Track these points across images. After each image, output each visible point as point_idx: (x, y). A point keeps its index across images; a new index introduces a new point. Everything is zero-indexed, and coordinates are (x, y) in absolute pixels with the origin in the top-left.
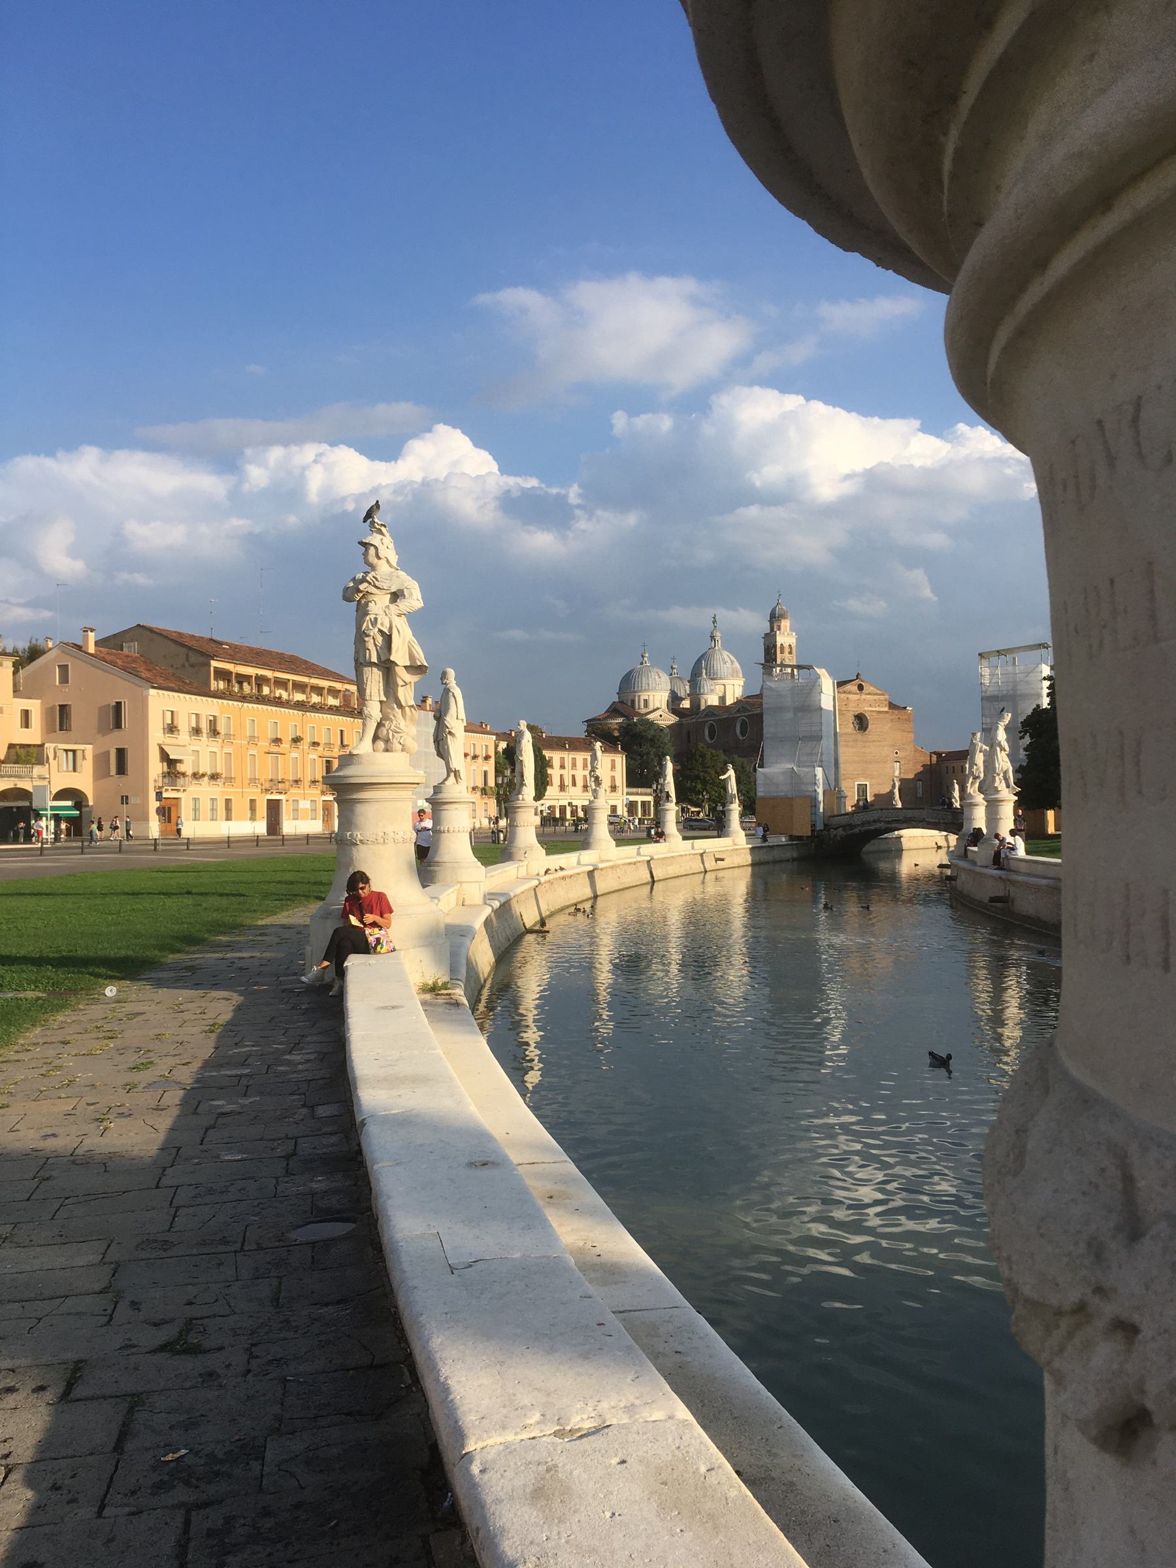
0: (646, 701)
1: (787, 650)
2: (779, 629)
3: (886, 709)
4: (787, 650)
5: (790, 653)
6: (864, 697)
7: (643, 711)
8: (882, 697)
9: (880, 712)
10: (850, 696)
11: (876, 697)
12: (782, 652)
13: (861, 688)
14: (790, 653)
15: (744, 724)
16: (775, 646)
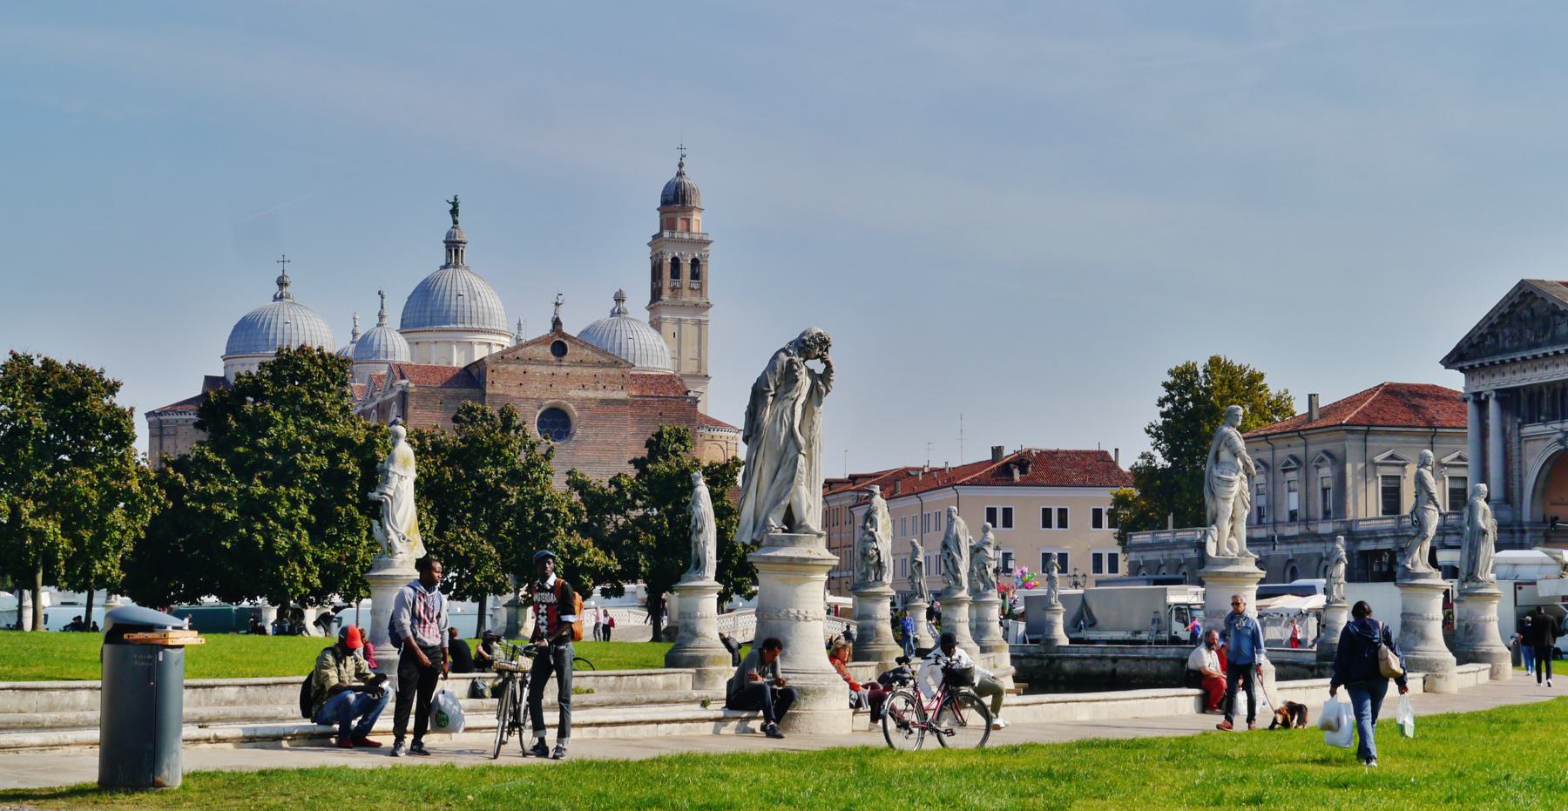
1: (686, 270)
4: (686, 270)
5: (695, 276)
6: (564, 370)
8: (613, 371)
10: (530, 368)
13: (559, 349)
14: (695, 276)
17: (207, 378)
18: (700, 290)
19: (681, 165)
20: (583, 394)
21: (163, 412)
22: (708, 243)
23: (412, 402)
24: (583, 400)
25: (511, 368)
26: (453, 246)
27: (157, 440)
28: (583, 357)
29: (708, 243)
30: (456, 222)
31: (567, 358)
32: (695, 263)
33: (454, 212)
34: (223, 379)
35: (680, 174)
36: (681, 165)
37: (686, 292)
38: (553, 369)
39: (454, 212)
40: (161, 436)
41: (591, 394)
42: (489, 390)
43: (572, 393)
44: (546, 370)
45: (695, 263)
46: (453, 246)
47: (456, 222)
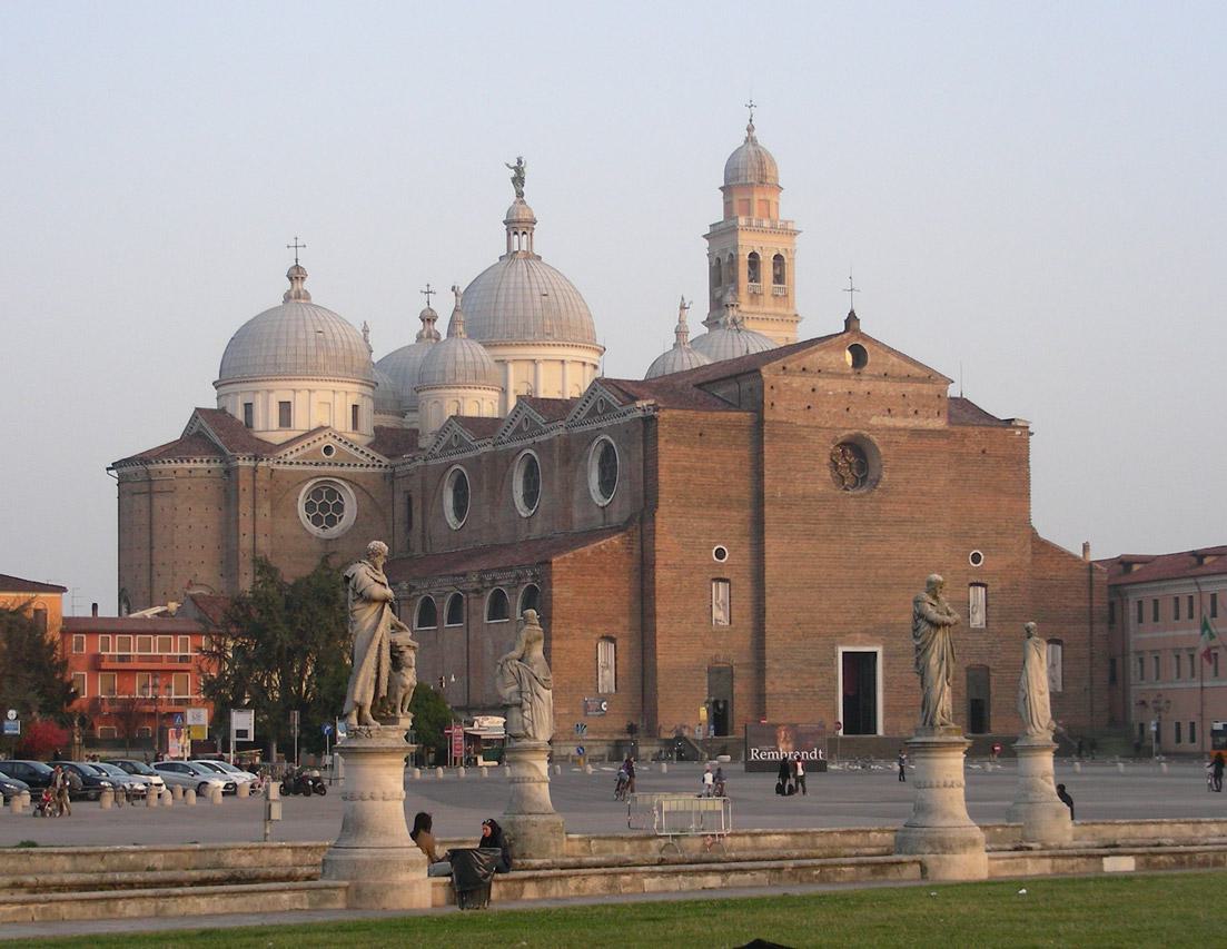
0: (285, 408)
1: (767, 270)
2: (748, 212)
3: (939, 423)
4: (767, 270)
5: (779, 278)
7: (278, 437)
8: (927, 389)
9: (917, 433)
10: (821, 383)
11: (910, 388)
12: (754, 275)
13: (859, 355)
14: (779, 279)
15: (531, 467)
16: (733, 260)
17: (197, 409)
18: (784, 298)
19: (750, 129)
20: (888, 421)
21: (143, 459)
22: (794, 233)
23: (664, 431)
24: (889, 429)
25: (797, 382)
26: (518, 224)
27: (142, 501)
28: (888, 369)
29: (794, 233)
30: (520, 195)
31: (866, 369)
32: (778, 258)
33: (518, 180)
34: (222, 411)
35: (750, 140)
36: (750, 129)
37: (768, 298)
38: (849, 385)
39: (518, 180)
40: (150, 493)
41: (900, 422)
42: (768, 416)
43: (874, 421)
44: (840, 386)
45: (778, 258)
46: (518, 224)
47: (520, 195)
